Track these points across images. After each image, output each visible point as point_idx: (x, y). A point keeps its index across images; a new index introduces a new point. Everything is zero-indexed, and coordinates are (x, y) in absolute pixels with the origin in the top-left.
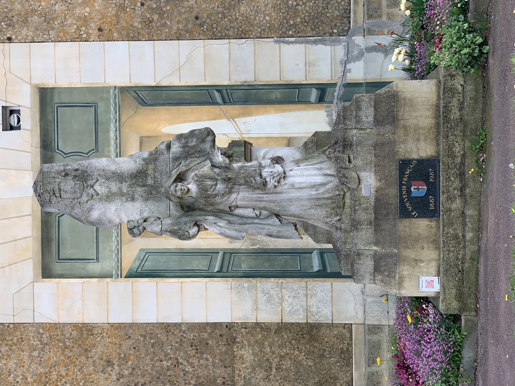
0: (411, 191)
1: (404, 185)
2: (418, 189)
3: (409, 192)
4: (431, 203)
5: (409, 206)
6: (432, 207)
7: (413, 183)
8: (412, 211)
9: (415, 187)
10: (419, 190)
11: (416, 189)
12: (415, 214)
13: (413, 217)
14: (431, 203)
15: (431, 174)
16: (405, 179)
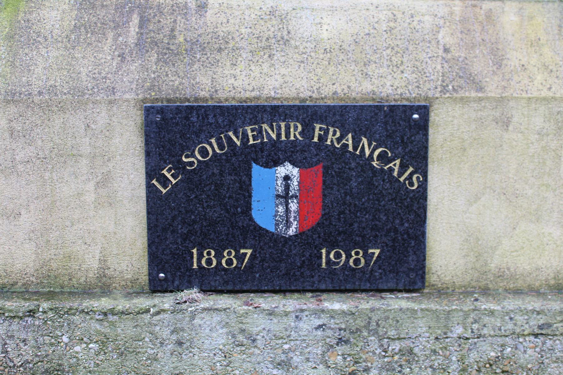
0: (277, 163)
1: (307, 131)
2: (285, 197)
3: (272, 156)
4: (219, 256)
5: (204, 152)
6: (202, 258)
7: (319, 170)
8: (179, 167)
9: (295, 183)
10: (277, 196)
11: (287, 188)
12: (164, 182)
13: (152, 173)
14: (219, 256)
15: (357, 254)
16: (332, 137)
